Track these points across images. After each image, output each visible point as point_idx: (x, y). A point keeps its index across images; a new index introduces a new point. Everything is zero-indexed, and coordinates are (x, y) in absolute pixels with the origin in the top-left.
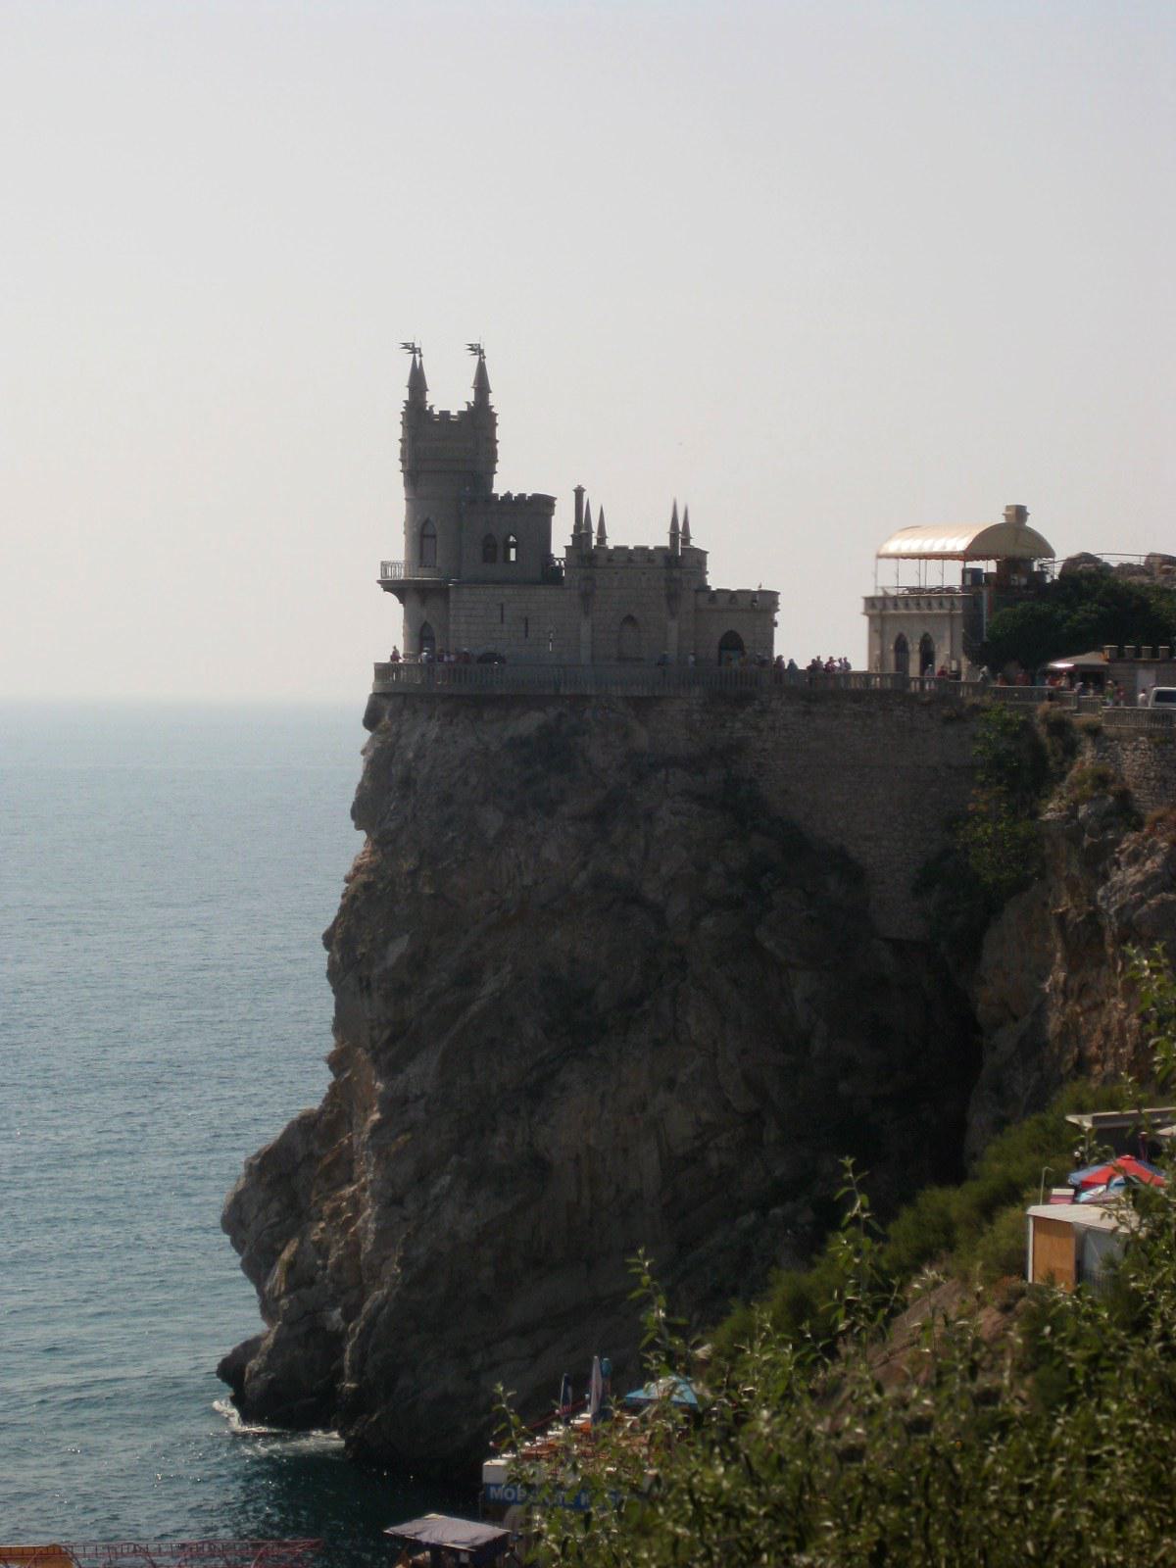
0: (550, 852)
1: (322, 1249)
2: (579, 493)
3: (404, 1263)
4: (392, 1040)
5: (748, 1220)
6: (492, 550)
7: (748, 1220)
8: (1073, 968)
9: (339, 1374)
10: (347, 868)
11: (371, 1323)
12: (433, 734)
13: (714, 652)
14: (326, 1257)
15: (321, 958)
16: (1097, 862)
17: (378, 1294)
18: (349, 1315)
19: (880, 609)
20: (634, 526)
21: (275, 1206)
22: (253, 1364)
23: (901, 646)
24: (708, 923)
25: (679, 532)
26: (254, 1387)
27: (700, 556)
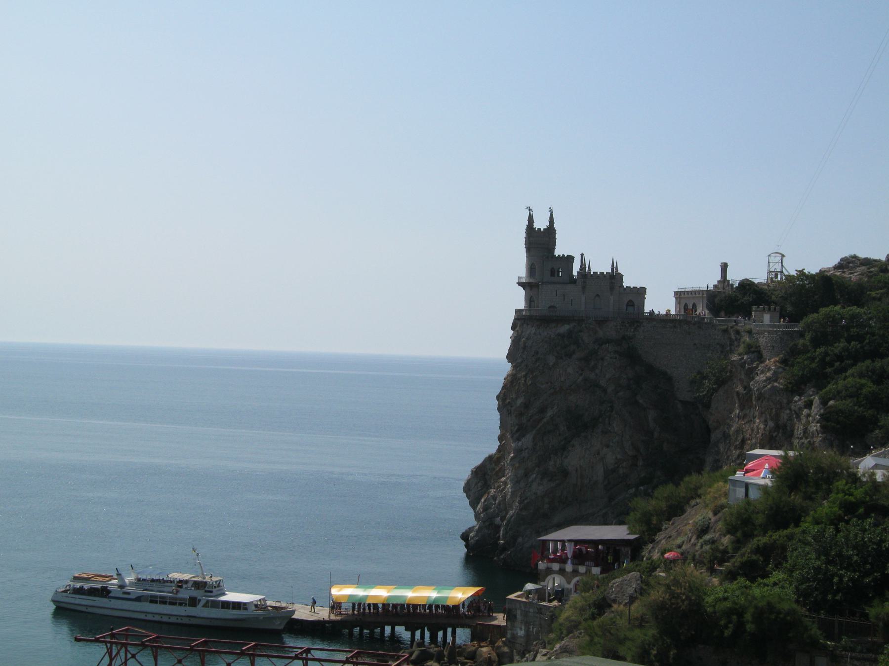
0: (570, 370)
1: (494, 498)
2: (582, 255)
3: (520, 503)
4: (517, 431)
5: (632, 491)
6: (553, 273)
7: (632, 491)
8: (741, 410)
9: (499, 538)
10: (505, 375)
11: (509, 521)
12: (534, 331)
13: (625, 307)
14: (495, 500)
15: (495, 403)
16: (751, 373)
17: (511, 512)
18: (503, 519)
19: (680, 296)
20: (600, 266)
21: (480, 484)
22: (472, 535)
23: (686, 305)
24: (621, 394)
25: (614, 267)
26: (472, 542)
27: (621, 276)
